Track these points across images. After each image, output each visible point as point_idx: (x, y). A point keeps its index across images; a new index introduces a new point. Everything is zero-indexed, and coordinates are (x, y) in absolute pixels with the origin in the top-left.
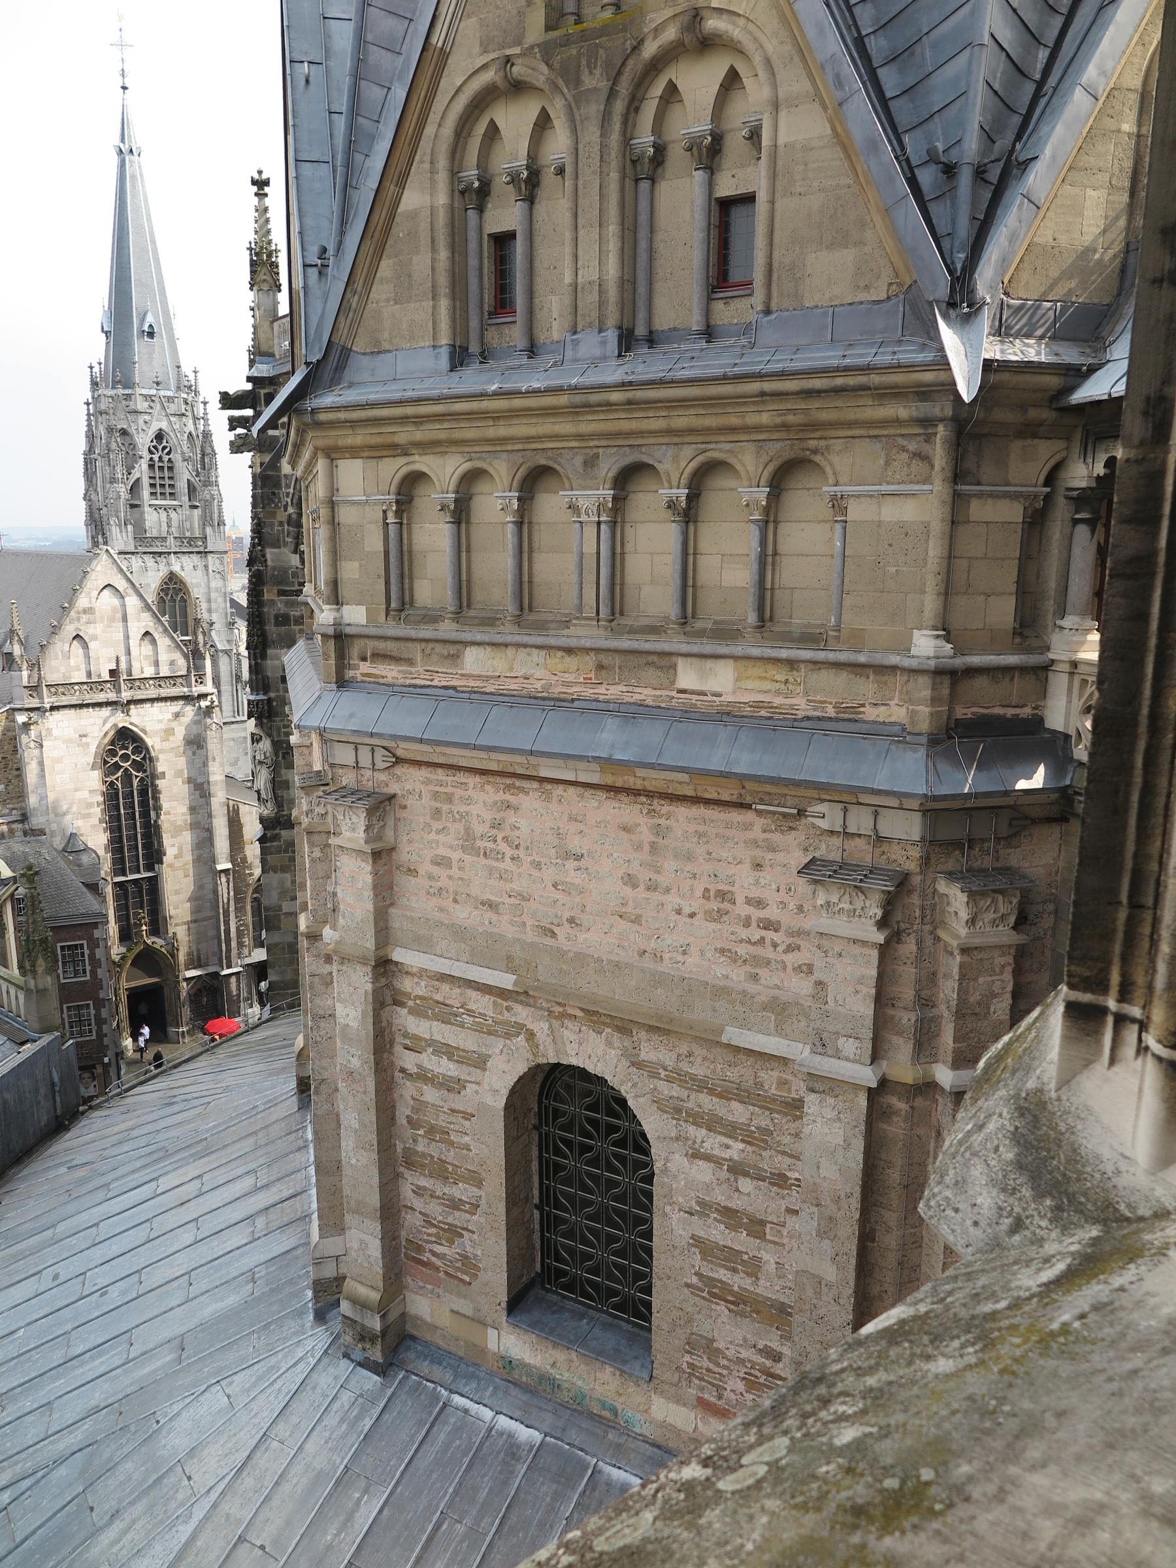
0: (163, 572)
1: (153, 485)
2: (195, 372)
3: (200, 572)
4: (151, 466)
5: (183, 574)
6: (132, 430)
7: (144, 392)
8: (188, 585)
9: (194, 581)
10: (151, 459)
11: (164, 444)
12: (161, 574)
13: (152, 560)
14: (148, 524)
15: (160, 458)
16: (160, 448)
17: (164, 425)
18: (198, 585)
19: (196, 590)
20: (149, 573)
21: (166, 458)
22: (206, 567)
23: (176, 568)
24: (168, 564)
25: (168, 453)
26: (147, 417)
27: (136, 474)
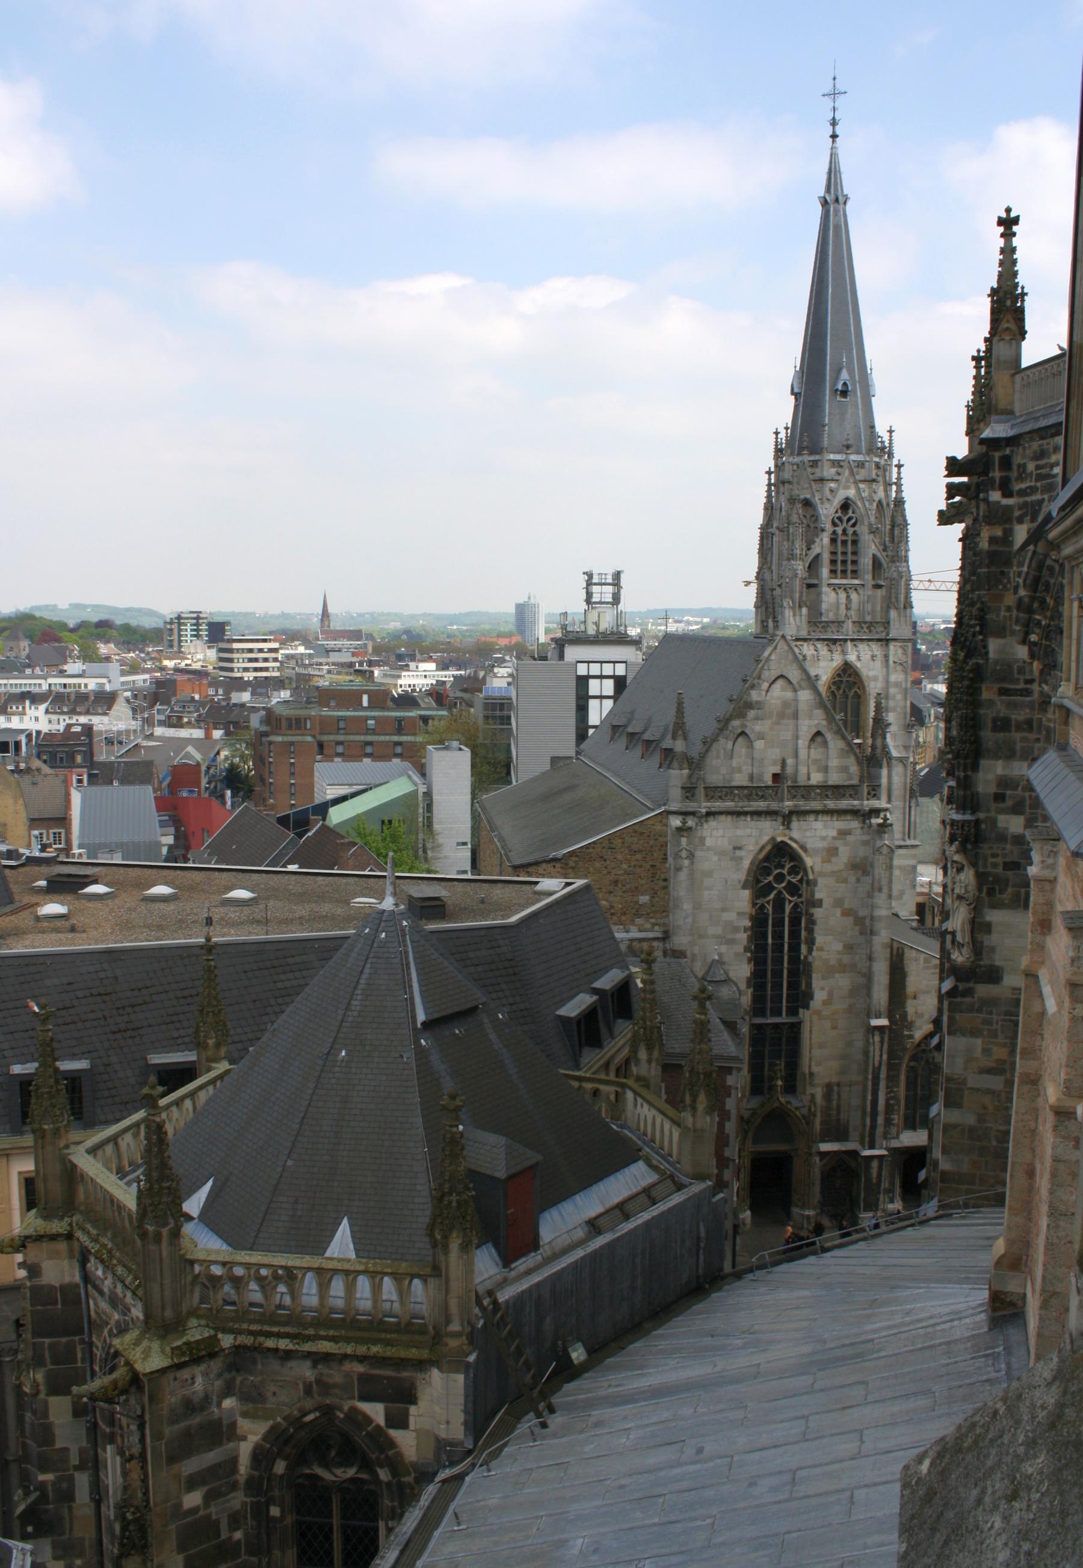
0: (837, 660)
1: (833, 562)
2: (891, 432)
3: (878, 664)
4: (833, 541)
5: (858, 665)
6: (816, 500)
7: (832, 457)
8: (864, 678)
9: (871, 674)
10: (834, 532)
11: (850, 514)
12: (835, 664)
13: (825, 648)
14: (824, 606)
15: (844, 531)
16: (845, 519)
17: (851, 493)
18: (876, 679)
20: (822, 664)
21: (850, 531)
22: (886, 656)
23: (852, 657)
24: (844, 652)
25: (854, 525)
26: (833, 485)
27: (816, 549)
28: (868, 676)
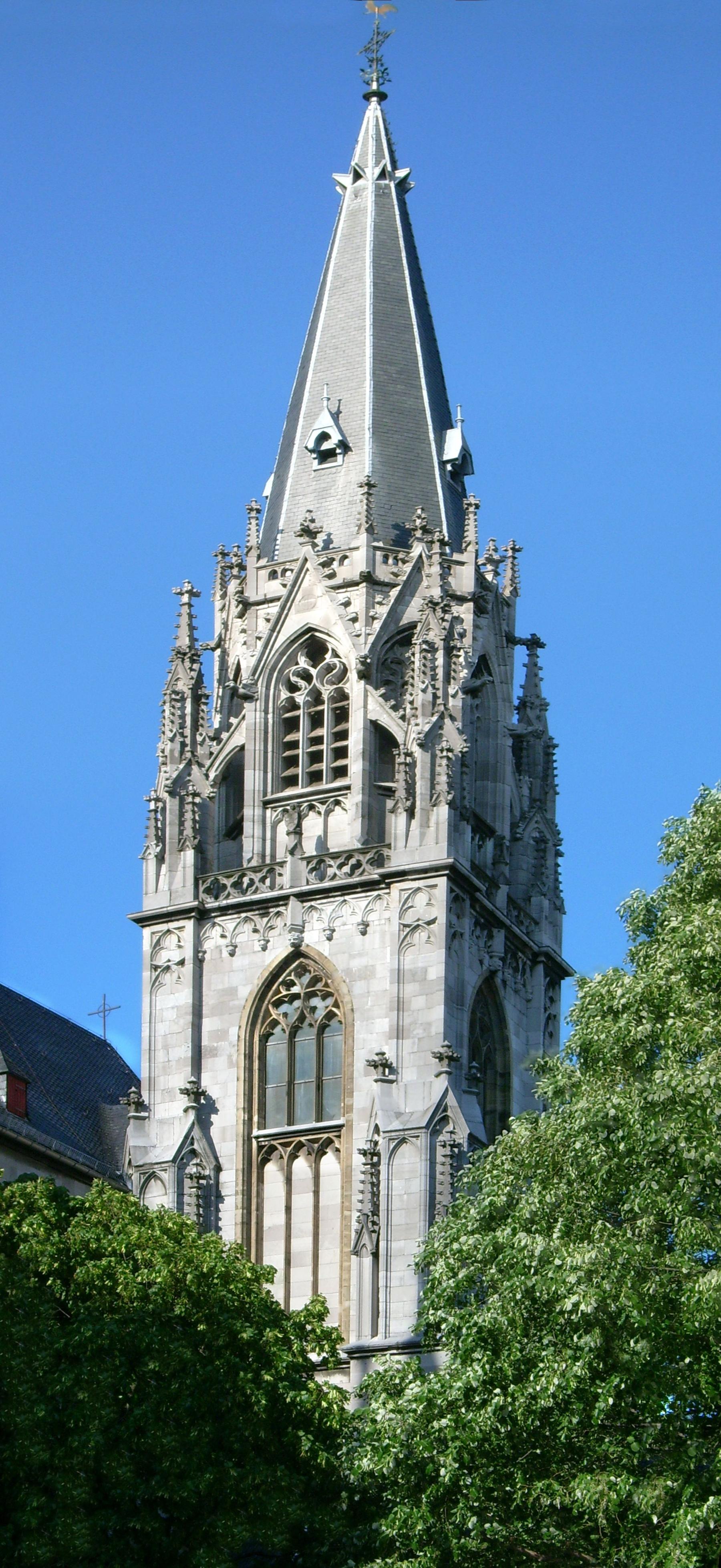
8: (339, 975)
9: (356, 964)
13: (248, 927)
18: (368, 973)
19: (359, 988)
28: (348, 971)
